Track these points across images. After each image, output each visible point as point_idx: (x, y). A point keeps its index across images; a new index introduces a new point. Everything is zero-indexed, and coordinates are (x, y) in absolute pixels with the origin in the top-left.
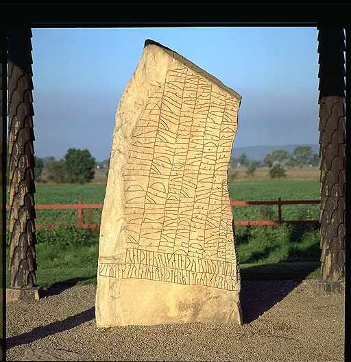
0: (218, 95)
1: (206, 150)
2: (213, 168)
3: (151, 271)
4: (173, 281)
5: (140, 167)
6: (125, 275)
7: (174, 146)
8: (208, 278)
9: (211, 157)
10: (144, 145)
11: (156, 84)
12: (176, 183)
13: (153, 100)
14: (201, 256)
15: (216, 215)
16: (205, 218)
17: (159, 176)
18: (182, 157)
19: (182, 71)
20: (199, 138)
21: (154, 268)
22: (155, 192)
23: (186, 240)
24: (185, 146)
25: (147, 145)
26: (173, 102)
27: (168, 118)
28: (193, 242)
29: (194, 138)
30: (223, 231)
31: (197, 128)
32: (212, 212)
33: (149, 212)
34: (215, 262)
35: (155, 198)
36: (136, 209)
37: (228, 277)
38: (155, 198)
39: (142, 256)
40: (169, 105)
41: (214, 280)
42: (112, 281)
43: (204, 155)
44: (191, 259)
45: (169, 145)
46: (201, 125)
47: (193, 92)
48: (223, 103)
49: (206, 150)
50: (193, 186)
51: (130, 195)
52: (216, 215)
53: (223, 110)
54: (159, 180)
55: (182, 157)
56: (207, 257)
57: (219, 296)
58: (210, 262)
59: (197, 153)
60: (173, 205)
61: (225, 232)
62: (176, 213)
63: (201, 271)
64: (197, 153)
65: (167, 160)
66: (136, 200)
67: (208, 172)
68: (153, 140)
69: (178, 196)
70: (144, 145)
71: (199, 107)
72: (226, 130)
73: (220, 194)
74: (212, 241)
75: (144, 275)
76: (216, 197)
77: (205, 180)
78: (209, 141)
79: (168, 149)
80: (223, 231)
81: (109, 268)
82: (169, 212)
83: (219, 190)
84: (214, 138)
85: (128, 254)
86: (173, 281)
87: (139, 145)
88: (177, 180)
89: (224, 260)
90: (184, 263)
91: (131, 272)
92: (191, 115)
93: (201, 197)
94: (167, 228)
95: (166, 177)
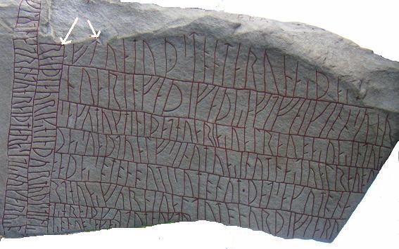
0: (342, 204)
1: (244, 185)
2: (209, 196)
4: (12, 127)
5: (211, 64)
6: (19, 44)
7: (249, 129)
9: (229, 194)
10: (250, 67)
16: (121, 181)
17: (194, 100)
20: (265, 173)
22: (164, 92)
23: (81, 148)
24: (250, 147)
25: (250, 77)
27: (302, 114)
28: (79, 162)
29: (265, 163)
31: (283, 167)
32: (132, 195)
33: (129, 83)
34: (47, 200)
37: (25, 221)
39: (51, 73)
41: (18, 196)
42: (11, 22)
43: (234, 181)
44: (49, 159)
45: (251, 118)
46: (289, 175)
47: (349, 159)
48: (328, 215)
49: (244, 185)
50: (177, 163)
51: (157, 48)
54: (186, 100)
58: (43, 192)
63: (30, 177)
66: (149, 58)
67: (203, 189)
69: (158, 133)
70: (250, 67)
71: (322, 170)
72: (280, 221)
73: (164, 208)
76: (158, 202)
78: (259, 192)
79: (244, 115)
81: (33, 15)
82: (129, 119)
83: (171, 207)
86: (12, 127)
87: (251, 61)
88: (188, 132)
91: (26, 53)
93: (157, 175)
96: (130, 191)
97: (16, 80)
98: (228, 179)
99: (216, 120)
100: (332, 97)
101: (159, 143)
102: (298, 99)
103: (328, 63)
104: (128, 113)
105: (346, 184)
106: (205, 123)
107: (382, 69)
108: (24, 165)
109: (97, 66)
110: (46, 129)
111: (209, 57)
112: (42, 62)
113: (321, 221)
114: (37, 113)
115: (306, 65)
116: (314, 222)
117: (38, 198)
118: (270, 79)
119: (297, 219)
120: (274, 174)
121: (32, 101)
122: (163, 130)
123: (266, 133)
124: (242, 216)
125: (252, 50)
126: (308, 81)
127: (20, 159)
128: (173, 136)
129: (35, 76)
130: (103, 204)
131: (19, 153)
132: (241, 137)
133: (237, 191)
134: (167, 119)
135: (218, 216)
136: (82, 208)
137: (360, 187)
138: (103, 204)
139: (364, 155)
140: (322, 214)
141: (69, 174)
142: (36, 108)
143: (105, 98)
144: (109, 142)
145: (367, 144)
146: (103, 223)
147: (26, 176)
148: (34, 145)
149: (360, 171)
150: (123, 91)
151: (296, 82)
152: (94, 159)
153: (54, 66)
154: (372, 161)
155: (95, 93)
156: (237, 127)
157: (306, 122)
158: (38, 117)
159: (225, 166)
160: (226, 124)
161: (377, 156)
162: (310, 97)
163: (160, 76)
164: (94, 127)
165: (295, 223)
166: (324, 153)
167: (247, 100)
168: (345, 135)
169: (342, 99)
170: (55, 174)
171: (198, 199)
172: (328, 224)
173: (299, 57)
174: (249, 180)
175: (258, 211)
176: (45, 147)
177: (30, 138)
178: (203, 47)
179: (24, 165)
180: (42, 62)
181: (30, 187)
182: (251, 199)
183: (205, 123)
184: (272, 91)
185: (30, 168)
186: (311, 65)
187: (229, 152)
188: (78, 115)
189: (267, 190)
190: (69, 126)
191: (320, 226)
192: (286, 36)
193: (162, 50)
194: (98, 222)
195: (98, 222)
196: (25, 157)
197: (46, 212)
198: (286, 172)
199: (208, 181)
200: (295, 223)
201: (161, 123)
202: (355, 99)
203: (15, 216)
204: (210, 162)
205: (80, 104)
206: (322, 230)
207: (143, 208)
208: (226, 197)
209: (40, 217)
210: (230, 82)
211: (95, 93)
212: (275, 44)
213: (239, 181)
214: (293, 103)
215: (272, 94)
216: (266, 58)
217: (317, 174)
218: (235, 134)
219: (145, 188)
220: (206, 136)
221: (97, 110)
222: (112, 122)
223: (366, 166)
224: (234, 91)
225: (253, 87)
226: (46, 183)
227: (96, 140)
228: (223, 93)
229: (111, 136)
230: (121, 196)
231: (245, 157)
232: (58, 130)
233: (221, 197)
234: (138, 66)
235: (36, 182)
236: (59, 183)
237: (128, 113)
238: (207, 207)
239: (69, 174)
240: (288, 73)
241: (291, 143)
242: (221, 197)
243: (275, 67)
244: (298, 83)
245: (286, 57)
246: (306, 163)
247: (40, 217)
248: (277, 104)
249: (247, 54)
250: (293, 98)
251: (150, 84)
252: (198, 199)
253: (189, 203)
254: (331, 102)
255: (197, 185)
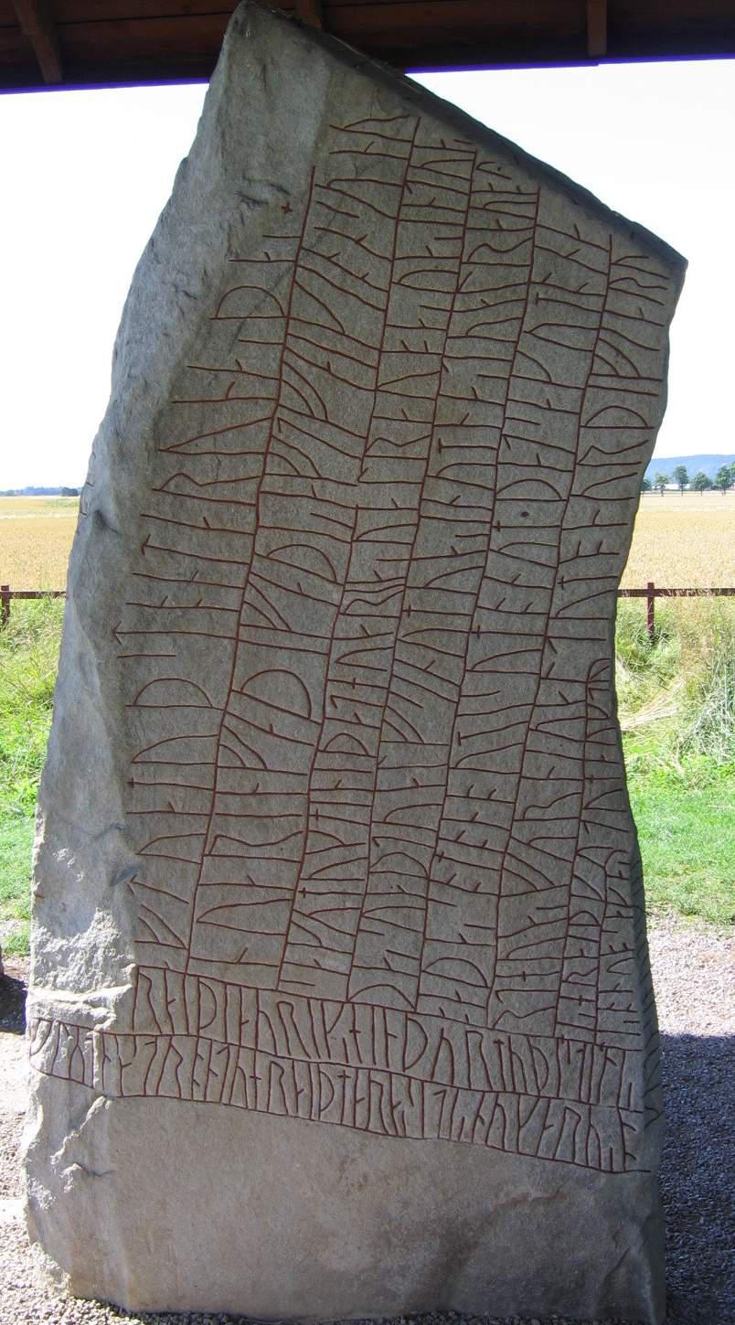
0: (569, 246)
1: (508, 514)
2: (539, 605)
3: (248, 1073)
6: (134, 1083)
8: (510, 1115)
9: (534, 553)
10: (208, 493)
11: (266, 194)
12: (360, 675)
13: (256, 276)
14: (476, 1017)
15: (555, 829)
18: (392, 552)
19: (388, 130)
20: (469, 456)
21: (262, 1062)
22: (261, 716)
23: (404, 942)
24: (408, 497)
25: (226, 492)
26: (349, 283)
27: (322, 358)
29: (451, 457)
30: (587, 905)
31: (462, 407)
33: (234, 805)
35: (261, 743)
36: (180, 793)
37: (605, 1108)
38: (261, 743)
39: (207, 1004)
40: (330, 296)
41: (534, 1123)
43: (498, 539)
44: (433, 1027)
48: (598, 284)
50: (448, 692)
52: (555, 829)
53: (593, 321)
54: (282, 660)
55: (392, 552)
56: (507, 1024)
57: (558, 1195)
58: (523, 1052)
59: (461, 529)
60: (348, 781)
61: (596, 909)
62: (361, 816)
63: (481, 1085)
64: (461, 529)
65: (319, 567)
67: (518, 624)
68: (254, 466)
69: (367, 736)
70: (208, 493)
72: (609, 418)
73: (575, 730)
74: (533, 952)
75: (214, 1084)
76: (554, 744)
77: (504, 665)
78: (528, 473)
79: (324, 510)
80: (587, 905)
82: (326, 810)
83: (568, 711)
84: (548, 458)
85: (141, 994)
86: (348, 1120)
87: (189, 488)
88: (364, 659)
89: (587, 1037)
90: (396, 1047)
91: (155, 1067)
92: (435, 341)
94: (323, 887)
95: (306, 643)
96: (523, 820)
97: (225, 1100)
98: (491, 556)
99: (335, 582)
100: (280, 278)
101: (393, 736)
102: (285, 368)
103: (196, 287)
104: (312, 811)
105: (512, 240)
106: (341, 612)
107: (218, 141)
108: (448, 1101)
109: (192, 883)
110: (354, 1031)
111: (175, 596)
112: (180, 1030)
113: (615, 303)
114: (310, 1050)
115: (198, 346)
116: (618, 325)
117: (540, 1070)
118: (232, 442)
119: (607, 369)
120: (479, 432)
121: (279, 1061)
122: (360, 723)
123: (371, 452)
124: (597, 522)
125: (158, 484)
126: (236, 340)
127: (433, 1108)
128: (375, 697)
129: (216, 1047)
130: (560, 896)
131: (417, 1109)
132: (382, 519)
133: (525, 532)
134: (329, 709)
135: (597, 586)
136: (571, 951)
137: (522, 199)
138: (560, 896)
139: (434, 191)
140: (595, 303)
141: (474, 978)
142: (297, 1054)
143: (273, 870)
144: (390, 866)
145: (406, 182)
146: (613, 898)
147: (478, 1096)
148: (395, 1066)
149: (478, 200)
150: (256, 821)
151: (241, 371)
152: (436, 913)
153: (191, 993)
154: (450, 168)
155: (261, 895)
156: (354, 529)
157: (343, 345)
158: (323, 1051)
159: (457, 563)
160: (345, 558)
161: (438, 155)
162: (277, 336)
163: (222, 725)
164: (348, 905)
165: (617, 376)
166: (426, 299)
167: (285, 501)
168: (381, 245)
169: (287, 250)
170: (476, 1017)
171: (547, 639)
172: (622, 285)
173: (179, 364)
174: (495, 500)
175: (583, 478)
176: (401, 1038)
177: (377, 1077)
178: (151, 610)
179: (448, 1101)
180: (180, 1030)
181: (509, 1088)
182: (549, 495)
183: (341, 612)
184: (264, 436)
185: (456, 1083)
186: (198, 333)
187: (419, 553)
188: (315, 943)
189: (524, 453)
190: (343, 969)
191: (630, 306)
192: (127, 397)
193: (156, 715)
194: (612, 910)
195: (612, 910)
196: (428, 1092)
197: (582, 1051)
198: (476, 399)
199: (497, 610)
200: (617, 376)
201: (340, 728)
202: (289, 217)
203: (592, 1132)
204: (445, 602)
205: (287, 935)
206: (640, 302)
207: (573, 787)
208: (543, 561)
209: (597, 1068)
210: (238, 542)
211: (261, 895)
212: (144, 425)
213: (498, 528)
214: (294, 380)
215: (271, 436)
216: (179, 450)
217: (483, 316)
218: (371, 536)
219: (514, 779)
220: (374, 610)
221: (304, 892)
222: (337, 855)
223: (467, 185)
224: (262, 534)
225: (251, 487)
226: (499, 1042)
227: (381, 901)
228: (267, 562)
229: (373, 861)
230: (539, 844)
231: (431, 510)
232: (354, 1000)
233: (544, 577)
234: (194, 781)
235: (497, 1069)
236: (502, 1007)
237: (312, 811)
238: (569, 613)
239: (474, 978)
240: (219, 395)
241: (397, 388)
242: (544, 577)
243: (201, 425)
244: (245, 368)
245: (177, 398)
246: (456, 348)
247: (597, 1068)
248: (298, 423)
249: (169, 499)
250: (280, 380)
251: (239, 749)
252: (547, 639)
253: (557, 660)
254: (294, 281)
255: (507, 639)
